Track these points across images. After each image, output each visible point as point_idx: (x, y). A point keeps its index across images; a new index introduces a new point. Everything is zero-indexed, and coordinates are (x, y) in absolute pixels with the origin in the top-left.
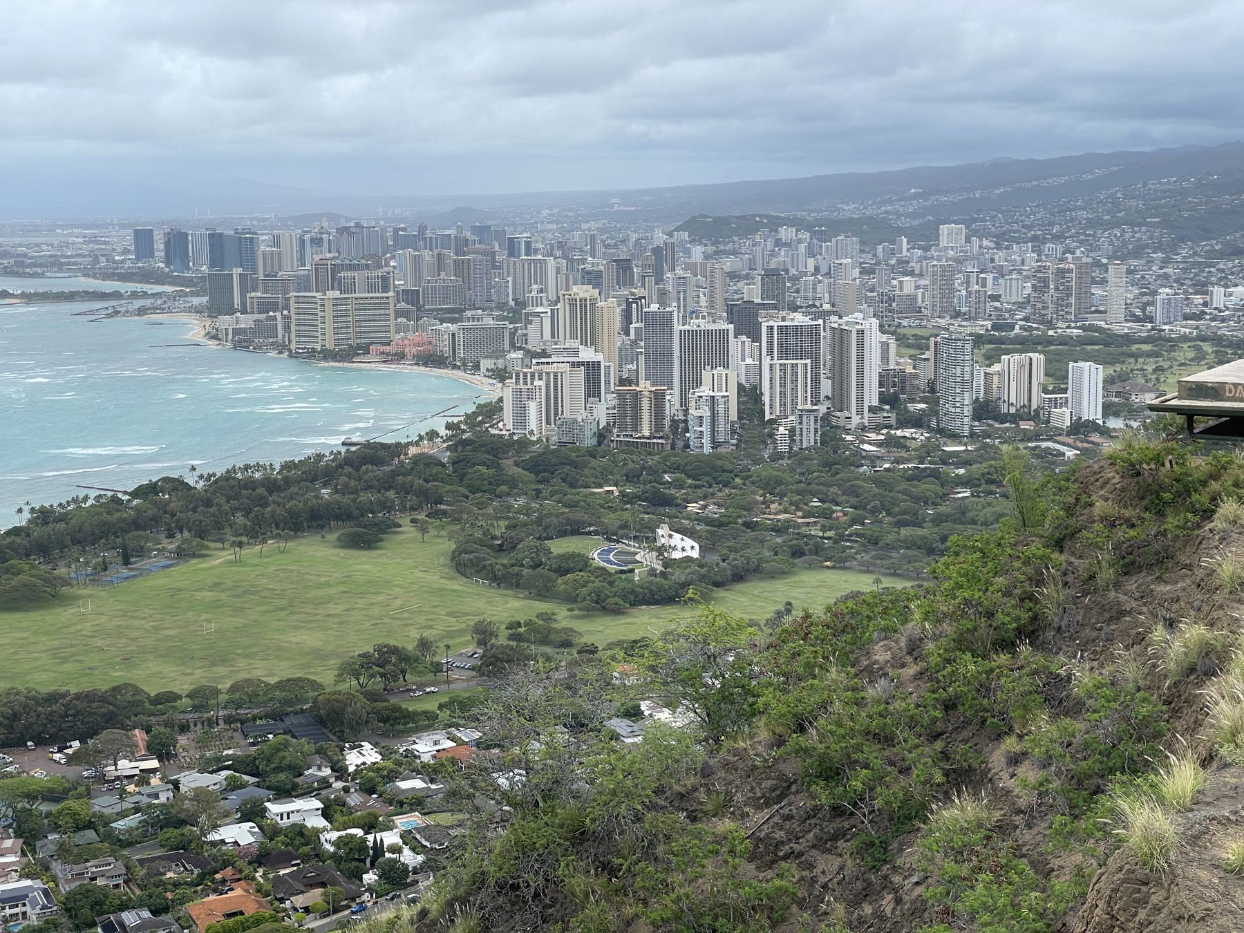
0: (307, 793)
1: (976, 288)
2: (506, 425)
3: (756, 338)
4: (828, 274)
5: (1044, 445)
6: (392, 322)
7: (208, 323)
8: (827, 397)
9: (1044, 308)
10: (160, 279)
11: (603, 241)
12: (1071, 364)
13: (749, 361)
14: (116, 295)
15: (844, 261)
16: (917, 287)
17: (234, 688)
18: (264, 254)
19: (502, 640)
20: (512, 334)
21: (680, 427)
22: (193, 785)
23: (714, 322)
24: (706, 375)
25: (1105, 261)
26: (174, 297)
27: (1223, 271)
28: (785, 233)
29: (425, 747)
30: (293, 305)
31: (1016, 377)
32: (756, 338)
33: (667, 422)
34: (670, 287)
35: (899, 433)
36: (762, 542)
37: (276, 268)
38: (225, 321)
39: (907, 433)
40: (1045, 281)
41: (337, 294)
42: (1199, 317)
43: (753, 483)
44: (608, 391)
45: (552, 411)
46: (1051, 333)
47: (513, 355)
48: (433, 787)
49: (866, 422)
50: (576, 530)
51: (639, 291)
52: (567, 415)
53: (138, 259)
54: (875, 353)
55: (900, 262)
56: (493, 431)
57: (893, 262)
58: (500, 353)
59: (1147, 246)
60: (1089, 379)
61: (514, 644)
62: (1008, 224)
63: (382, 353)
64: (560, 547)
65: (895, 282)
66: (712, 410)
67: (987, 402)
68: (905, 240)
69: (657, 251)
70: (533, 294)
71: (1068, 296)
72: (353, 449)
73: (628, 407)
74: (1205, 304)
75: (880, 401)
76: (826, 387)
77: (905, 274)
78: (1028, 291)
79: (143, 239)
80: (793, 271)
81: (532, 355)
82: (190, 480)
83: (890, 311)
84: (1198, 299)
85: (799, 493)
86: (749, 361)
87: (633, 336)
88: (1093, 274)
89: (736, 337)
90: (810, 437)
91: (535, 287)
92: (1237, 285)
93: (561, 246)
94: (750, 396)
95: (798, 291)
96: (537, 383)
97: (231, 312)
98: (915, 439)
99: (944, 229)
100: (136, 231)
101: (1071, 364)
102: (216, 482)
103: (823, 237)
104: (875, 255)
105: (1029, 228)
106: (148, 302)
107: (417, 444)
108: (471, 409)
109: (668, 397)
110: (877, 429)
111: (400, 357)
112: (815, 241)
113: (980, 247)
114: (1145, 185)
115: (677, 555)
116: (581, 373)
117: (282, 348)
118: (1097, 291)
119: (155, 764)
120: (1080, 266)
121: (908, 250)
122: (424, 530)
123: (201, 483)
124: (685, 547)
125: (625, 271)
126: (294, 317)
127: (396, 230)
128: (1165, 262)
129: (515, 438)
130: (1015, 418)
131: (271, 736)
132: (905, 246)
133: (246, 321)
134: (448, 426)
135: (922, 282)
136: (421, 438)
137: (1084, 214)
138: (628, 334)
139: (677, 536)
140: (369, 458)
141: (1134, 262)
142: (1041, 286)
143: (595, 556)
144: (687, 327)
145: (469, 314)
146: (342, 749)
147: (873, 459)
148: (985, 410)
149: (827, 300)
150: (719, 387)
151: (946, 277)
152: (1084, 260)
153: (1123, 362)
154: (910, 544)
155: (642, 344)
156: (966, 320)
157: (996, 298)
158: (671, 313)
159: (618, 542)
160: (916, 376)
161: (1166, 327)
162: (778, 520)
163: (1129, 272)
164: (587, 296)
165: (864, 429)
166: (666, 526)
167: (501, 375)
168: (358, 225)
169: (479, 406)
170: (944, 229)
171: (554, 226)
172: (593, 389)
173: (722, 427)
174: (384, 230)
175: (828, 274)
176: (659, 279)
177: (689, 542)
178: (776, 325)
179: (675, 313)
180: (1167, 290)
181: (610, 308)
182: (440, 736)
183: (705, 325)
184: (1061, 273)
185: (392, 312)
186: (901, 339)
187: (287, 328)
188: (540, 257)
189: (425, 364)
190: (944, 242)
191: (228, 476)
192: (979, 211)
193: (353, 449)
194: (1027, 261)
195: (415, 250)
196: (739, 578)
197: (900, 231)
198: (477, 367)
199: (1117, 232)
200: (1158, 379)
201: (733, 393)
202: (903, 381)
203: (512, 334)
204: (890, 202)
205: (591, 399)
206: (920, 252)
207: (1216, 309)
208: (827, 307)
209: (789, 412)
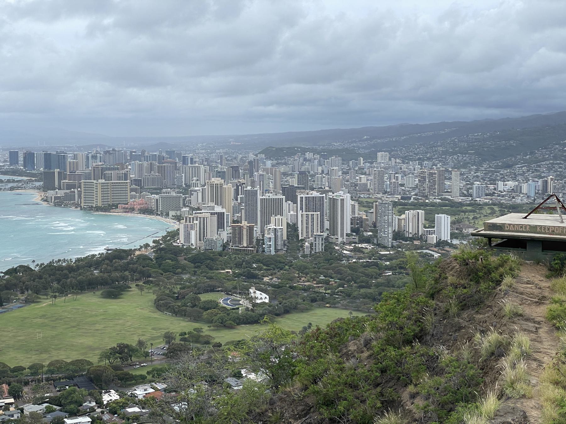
0: (83, 414)
1: (394, 180)
2: (181, 241)
3: (295, 202)
4: (328, 174)
5: (425, 251)
6: (129, 194)
8: (327, 229)
9: (424, 190)
10: (21, 174)
11: (226, 158)
12: (436, 215)
13: (292, 213)
15: (335, 168)
16: (368, 180)
17: (50, 364)
18: (70, 163)
19: (177, 341)
20: (184, 200)
21: (260, 242)
22: (30, 411)
23: (276, 195)
24: (273, 219)
25: (450, 169)
26: (27, 182)
27: (502, 174)
28: (308, 155)
29: (140, 392)
30: (82, 186)
31: (412, 221)
32: (295, 202)
33: (255, 240)
34: (256, 179)
35: (360, 246)
36: (298, 295)
37: (75, 169)
38: (51, 193)
39: (363, 245)
40: (424, 178)
41: (103, 181)
42: (492, 194)
43: (294, 268)
45: (202, 235)
46: (427, 201)
47: (184, 209)
48: (144, 411)
49: (345, 240)
50: (212, 289)
52: (209, 237)
53: (11, 165)
54: (349, 209)
55: (360, 169)
56: (175, 244)
57: (357, 169)
58: (178, 209)
59: (468, 163)
60: (444, 222)
61: (183, 343)
62: (408, 152)
63: (124, 208)
64: (204, 297)
65: (357, 178)
66: (275, 235)
67: (399, 232)
68: (362, 159)
69: (250, 163)
70: (194, 181)
71: (435, 185)
72: (109, 252)
73: (237, 233)
74: (495, 189)
75: (351, 231)
76: (327, 224)
77: (362, 174)
78: (417, 182)
79: (14, 156)
80: (312, 172)
81: (193, 209)
82: (32, 267)
83: (355, 190)
84: (492, 187)
85: (314, 273)
86: (292, 213)
87: (239, 201)
88: (445, 175)
89: (286, 202)
90: (319, 248)
91: (195, 178)
92: (508, 181)
93: (207, 160)
94: (292, 228)
95: (314, 181)
96: (195, 222)
98: (367, 248)
99: (379, 154)
100: (10, 153)
101: (436, 215)
102: (45, 267)
103: (325, 157)
104: (349, 166)
105: (417, 154)
106: (15, 185)
107: (139, 250)
108: (165, 234)
109: (255, 229)
110: (350, 244)
111: (132, 210)
112: (322, 159)
113: (395, 162)
114: (467, 136)
115: (258, 301)
116: (215, 217)
117: (77, 205)
118: (447, 183)
119: (12, 400)
120: (439, 172)
121: (363, 163)
122: (141, 288)
123: (38, 268)
124: (262, 298)
125: (236, 171)
126: (83, 191)
127: (131, 152)
128: (477, 170)
129: (185, 247)
130: (412, 239)
131: (67, 387)
132: (362, 162)
133: (61, 193)
134: (154, 242)
135: (370, 178)
136: (141, 247)
137: (441, 149)
138: (237, 200)
139: (258, 292)
140: (116, 257)
141: (463, 170)
142: (422, 180)
143: (221, 301)
144: (264, 197)
145: (164, 190)
146: (101, 393)
147: (348, 258)
148: (398, 235)
149: (327, 185)
150: (278, 224)
151: (381, 175)
152: (441, 169)
153: (459, 215)
154: (365, 296)
155: (244, 204)
156: (389, 195)
157: (402, 185)
158: (256, 191)
159: (232, 295)
160: (367, 220)
161: (478, 199)
162: (305, 285)
163: (461, 174)
164: (219, 182)
165: (344, 244)
166: (254, 288)
167: (178, 218)
168: (114, 150)
169: (168, 232)
170: (379, 154)
171: (204, 151)
172: (221, 225)
173: (279, 242)
174: (126, 152)
175: (328, 174)
176: (252, 175)
177: (264, 295)
178: (304, 196)
179: (259, 191)
180: (478, 183)
181: (229, 188)
182: (147, 386)
183: (272, 196)
184: (431, 174)
185: (129, 189)
186: (360, 203)
187: (80, 197)
188: (197, 165)
189: (144, 213)
190: (379, 160)
191: (50, 264)
192: (395, 147)
193: (109, 252)
194: (416, 169)
195: (140, 161)
196: (287, 311)
197: (360, 155)
198: (167, 215)
199: (456, 157)
200: (474, 222)
201: (284, 227)
202: (362, 222)
203: (184, 200)
204: (355, 142)
206: (369, 165)
207: (499, 191)
208: (327, 188)
209: (310, 236)
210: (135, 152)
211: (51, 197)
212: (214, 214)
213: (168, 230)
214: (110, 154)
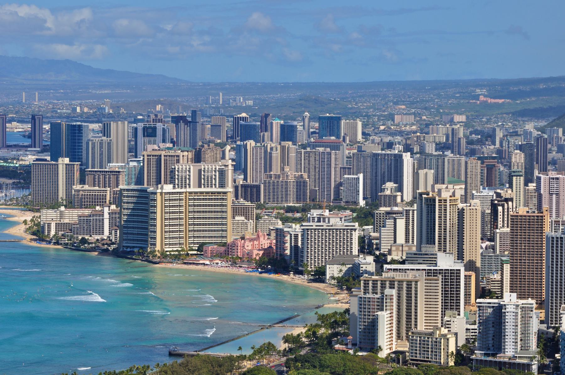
6: (229, 220)
7: (28, 216)
38: (49, 216)
41: (168, 188)
44: (467, 302)
51: (506, 193)
52: (421, 327)
96: (388, 291)
97: (55, 206)
107: (250, 358)
133: (71, 216)
134: (287, 339)
138: (492, 239)
145: (315, 213)
169: (323, 318)
172: (451, 302)
205: (448, 312)
210: (244, 119)
211: (49, 225)
212: (436, 273)
213: (321, 312)
214: (186, 122)
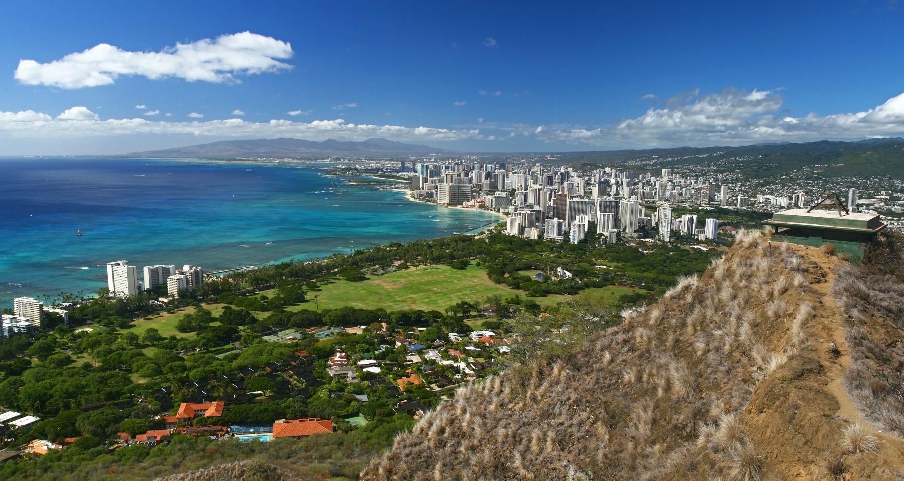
7: (411, 192)
14: (384, 182)
21: (567, 234)
24: (577, 217)
28: (608, 170)
64: (523, 273)
69: (562, 174)
94: (592, 225)
99: (663, 170)
